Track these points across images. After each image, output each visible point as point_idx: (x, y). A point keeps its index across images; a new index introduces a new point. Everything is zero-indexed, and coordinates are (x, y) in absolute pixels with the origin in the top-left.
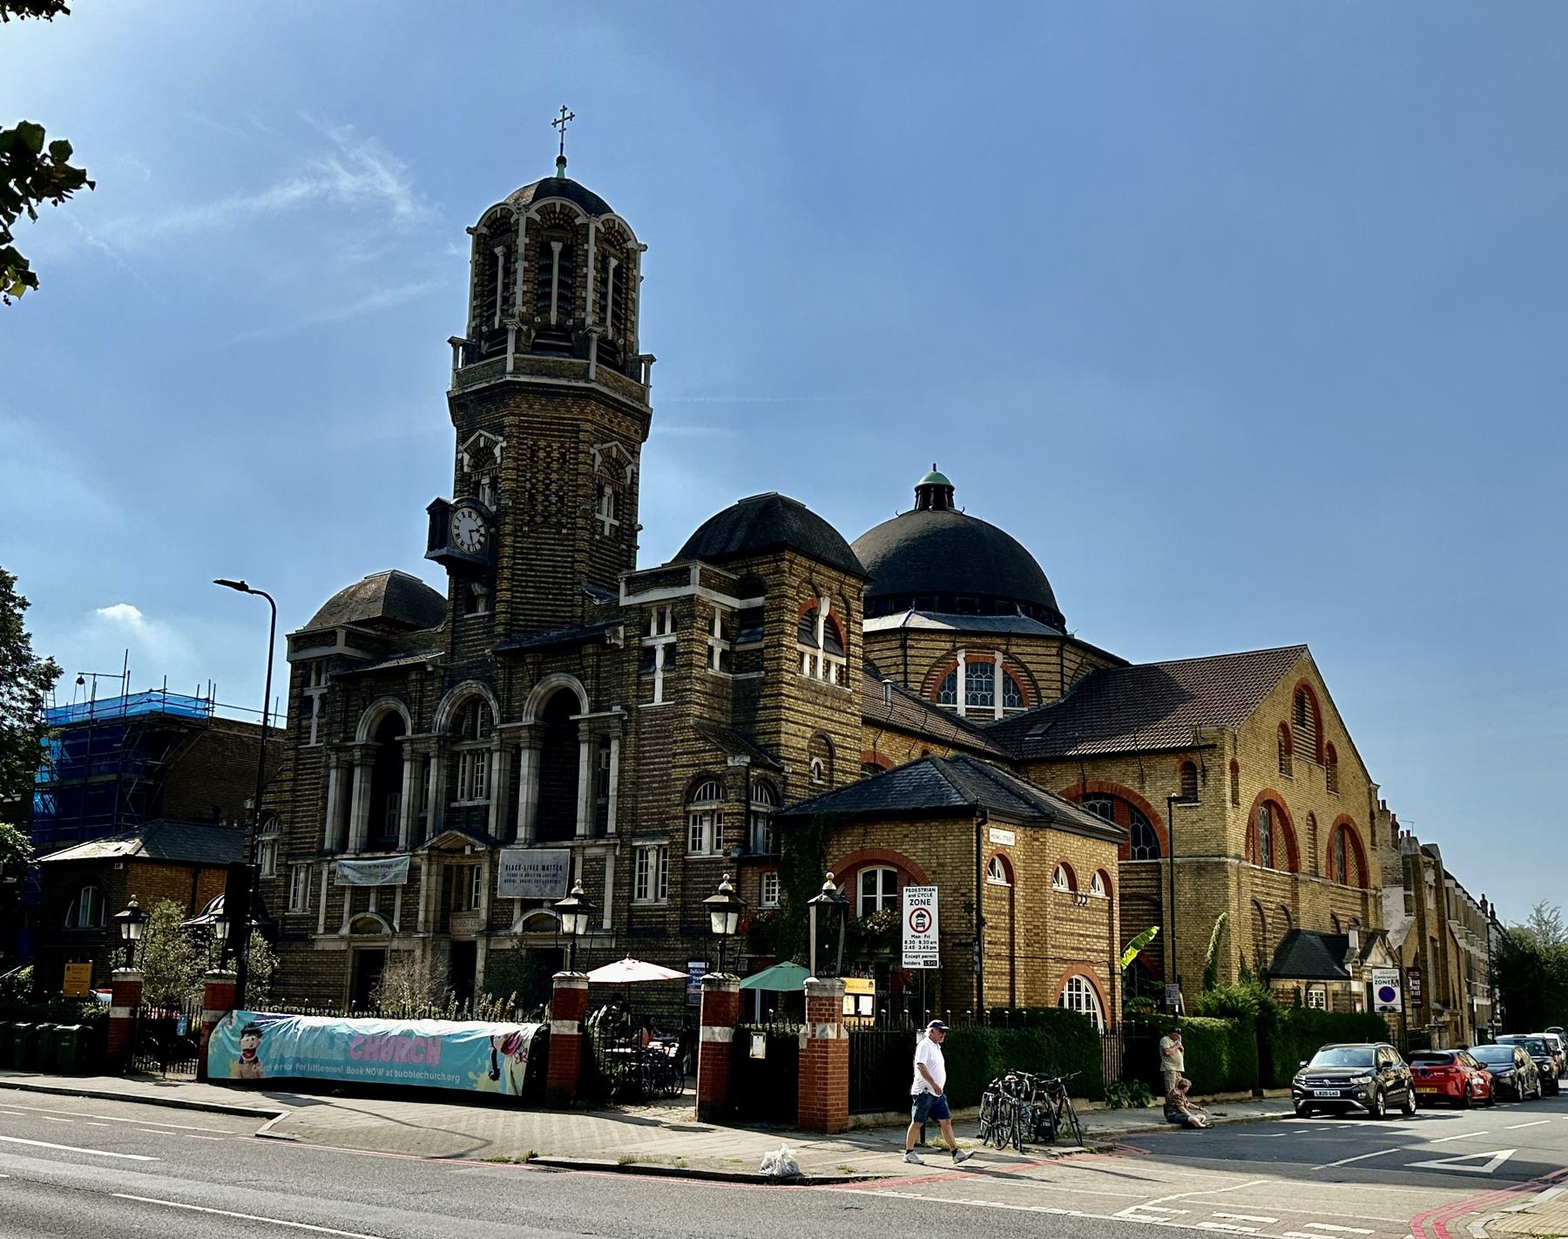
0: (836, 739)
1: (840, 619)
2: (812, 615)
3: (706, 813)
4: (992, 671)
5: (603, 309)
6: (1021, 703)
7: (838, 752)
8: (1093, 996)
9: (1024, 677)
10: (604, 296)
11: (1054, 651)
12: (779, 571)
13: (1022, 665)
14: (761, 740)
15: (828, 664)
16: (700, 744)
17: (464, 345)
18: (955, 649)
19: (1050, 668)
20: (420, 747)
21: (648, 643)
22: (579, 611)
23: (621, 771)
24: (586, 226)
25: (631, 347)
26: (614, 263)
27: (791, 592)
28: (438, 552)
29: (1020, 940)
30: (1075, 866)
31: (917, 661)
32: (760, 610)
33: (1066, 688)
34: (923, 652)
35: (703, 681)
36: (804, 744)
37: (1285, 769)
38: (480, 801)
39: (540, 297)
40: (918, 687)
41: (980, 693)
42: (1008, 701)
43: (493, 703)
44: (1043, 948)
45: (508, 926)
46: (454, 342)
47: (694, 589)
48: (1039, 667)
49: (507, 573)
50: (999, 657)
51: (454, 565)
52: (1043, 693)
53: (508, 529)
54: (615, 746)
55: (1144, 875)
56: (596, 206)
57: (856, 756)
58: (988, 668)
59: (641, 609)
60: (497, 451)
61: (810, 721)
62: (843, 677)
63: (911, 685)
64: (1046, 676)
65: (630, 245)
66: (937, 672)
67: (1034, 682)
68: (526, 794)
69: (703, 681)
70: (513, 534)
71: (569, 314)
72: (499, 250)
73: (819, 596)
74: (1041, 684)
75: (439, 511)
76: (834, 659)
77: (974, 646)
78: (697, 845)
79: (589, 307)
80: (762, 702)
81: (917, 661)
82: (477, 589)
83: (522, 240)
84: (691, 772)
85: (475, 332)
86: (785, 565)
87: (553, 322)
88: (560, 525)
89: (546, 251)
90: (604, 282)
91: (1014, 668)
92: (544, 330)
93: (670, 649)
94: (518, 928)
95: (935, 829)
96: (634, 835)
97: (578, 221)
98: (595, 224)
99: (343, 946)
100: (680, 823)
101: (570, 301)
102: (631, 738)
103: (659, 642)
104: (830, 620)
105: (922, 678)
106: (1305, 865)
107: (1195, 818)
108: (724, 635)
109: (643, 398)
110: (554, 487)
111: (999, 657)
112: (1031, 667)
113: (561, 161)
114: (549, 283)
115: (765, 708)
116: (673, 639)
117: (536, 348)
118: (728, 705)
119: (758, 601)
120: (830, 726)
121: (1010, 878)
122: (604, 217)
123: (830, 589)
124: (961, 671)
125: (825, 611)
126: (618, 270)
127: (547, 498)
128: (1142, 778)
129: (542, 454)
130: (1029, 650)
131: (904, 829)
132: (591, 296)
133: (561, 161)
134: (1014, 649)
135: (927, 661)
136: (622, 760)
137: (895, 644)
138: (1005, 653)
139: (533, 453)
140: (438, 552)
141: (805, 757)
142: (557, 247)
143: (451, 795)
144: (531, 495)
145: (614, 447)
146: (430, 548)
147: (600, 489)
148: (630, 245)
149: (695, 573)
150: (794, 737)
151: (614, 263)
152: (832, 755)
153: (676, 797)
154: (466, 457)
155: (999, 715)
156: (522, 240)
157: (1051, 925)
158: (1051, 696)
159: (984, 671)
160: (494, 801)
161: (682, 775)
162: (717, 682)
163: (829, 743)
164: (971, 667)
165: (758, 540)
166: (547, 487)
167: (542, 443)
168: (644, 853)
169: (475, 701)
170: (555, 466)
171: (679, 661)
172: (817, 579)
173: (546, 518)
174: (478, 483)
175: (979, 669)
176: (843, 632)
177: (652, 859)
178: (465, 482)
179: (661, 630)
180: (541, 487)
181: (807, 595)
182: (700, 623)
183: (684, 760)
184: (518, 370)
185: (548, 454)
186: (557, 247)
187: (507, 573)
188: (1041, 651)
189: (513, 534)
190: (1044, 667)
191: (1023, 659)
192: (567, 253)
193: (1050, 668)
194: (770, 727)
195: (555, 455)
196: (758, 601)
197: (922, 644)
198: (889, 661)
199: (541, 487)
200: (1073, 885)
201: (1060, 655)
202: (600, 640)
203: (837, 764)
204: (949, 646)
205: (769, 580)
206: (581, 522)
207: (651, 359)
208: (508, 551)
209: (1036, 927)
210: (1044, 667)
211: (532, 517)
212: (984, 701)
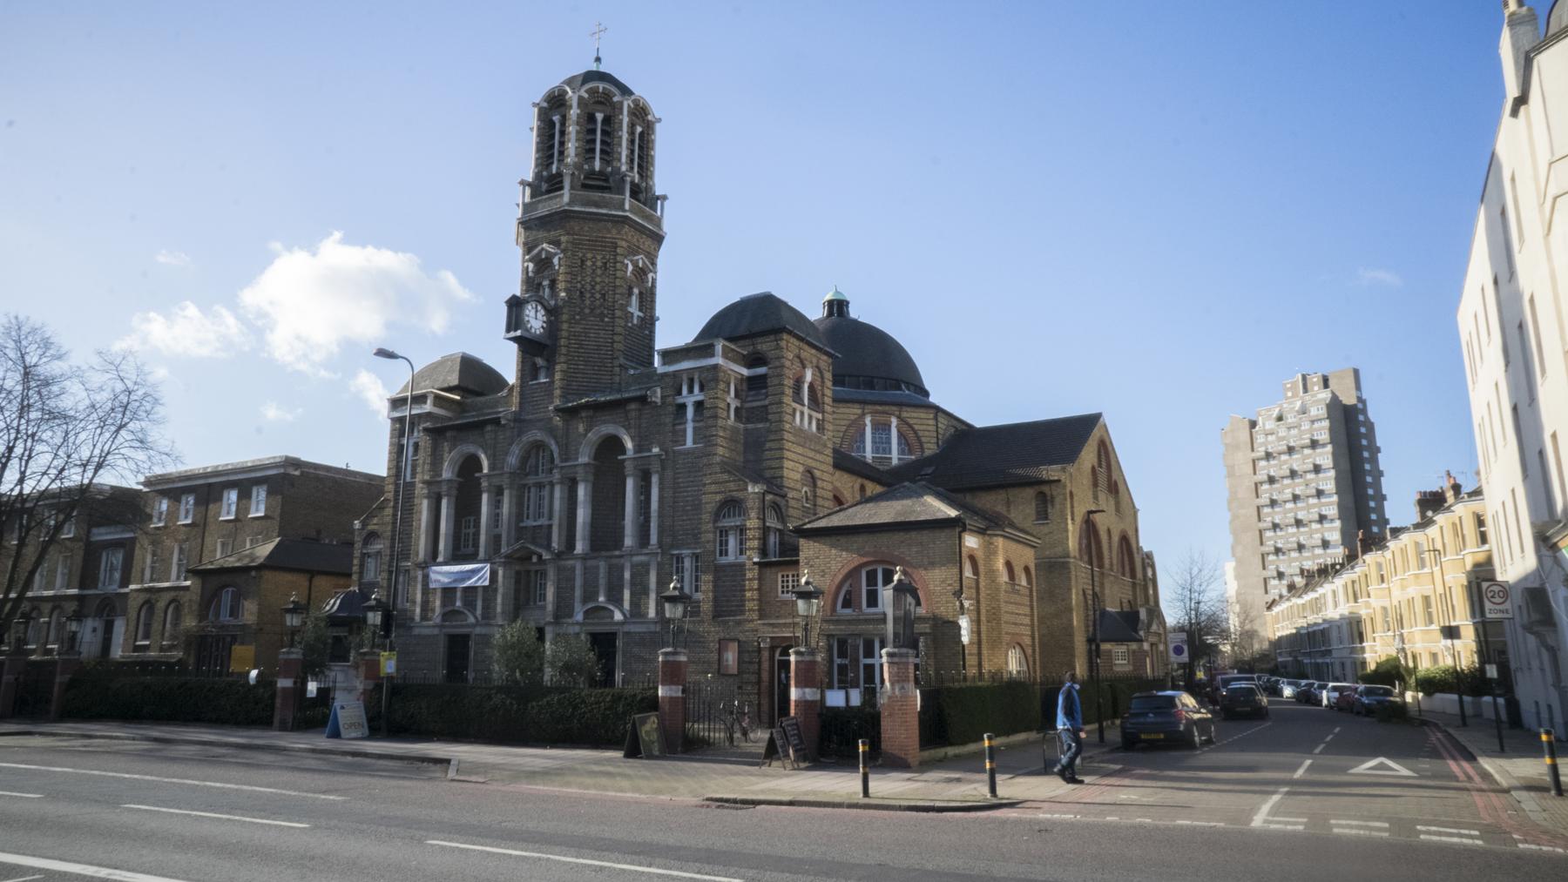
0: (817, 473)
2: (798, 382)
3: (731, 528)
5: (632, 161)
6: (910, 453)
7: (819, 483)
10: (632, 151)
12: (779, 348)
13: (910, 426)
14: (768, 474)
15: (810, 417)
16: (726, 477)
17: (529, 185)
18: (864, 414)
20: (496, 481)
21: (680, 400)
22: (617, 379)
23: (661, 498)
24: (621, 103)
25: (649, 189)
26: (639, 129)
27: (788, 363)
28: (512, 334)
29: (983, 618)
30: (1014, 564)
32: (763, 377)
35: (724, 429)
36: (798, 476)
37: (1096, 498)
38: (543, 521)
39: (587, 152)
41: (882, 444)
42: (901, 452)
43: (554, 447)
44: (999, 624)
45: (571, 616)
46: (523, 183)
47: (718, 360)
50: (894, 421)
51: (528, 347)
53: (565, 317)
56: (626, 91)
57: (830, 487)
59: (675, 374)
60: (556, 261)
61: (802, 460)
62: (820, 427)
66: (852, 430)
67: (918, 438)
68: (582, 515)
69: (724, 429)
70: (569, 322)
72: (556, 118)
73: (804, 367)
75: (515, 305)
76: (815, 414)
77: (877, 412)
78: (724, 552)
80: (768, 445)
82: (540, 361)
83: (574, 112)
84: (719, 497)
85: (538, 176)
86: (783, 344)
89: (591, 118)
91: (905, 428)
92: (591, 174)
93: (699, 405)
94: (579, 617)
95: (925, 536)
96: (673, 547)
97: (615, 99)
98: (627, 103)
99: (436, 631)
100: (711, 536)
101: (608, 153)
102: (669, 473)
103: (689, 399)
104: (811, 386)
106: (1107, 562)
108: (737, 396)
109: (659, 225)
111: (894, 421)
113: (598, 59)
114: (594, 141)
116: (700, 398)
117: (585, 187)
118: (741, 448)
119: (762, 370)
120: (813, 464)
124: (868, 430)
126: (642, 134)
128: (1008, 504)
129: (589, 263)
131: (898, 537)
132: (624, 153)
133: (598, 59)
134: (904, 415)
136: (661, 490)
138: (899, 417)
140: (512, 334)
141: (798, 486)
142: (599, 116)
143: (519, 515)
145: (641, 260)
146: (508, 331)
147: (630, 289)
149: (719, 347)
150: (792, 472)
151: (639, 129)
152: (815, 485)
153: (706, 517)
154: (531, 266)
155: (895, 462)
156: (574, 112)
157: (1004, 608)
158: (931, 449)
160: (556, 522)
161: (711, 500)
162: (734, 430)
163: (813, 478)
165: (754, 324)
166: (593, 287)
167: (589, 255)
168: (680, 559)
169: (539, 446)
170: (599, 272)
171: (707, 413)
172: (804, 355)
174: (540, 284)
175: (881, 428)
177: (687, 563)
178: (531, 283)
179: (691, 391)
180: (588, 287)
181: (797, 364)
182: (722, 386)
183: (713, 488)
184: (571, 202)
186: (599, 116)
187: (564, 350)
189: (569, 322)
192: (607, 120)
194: (774, 464)
195: (599, 264)
196: (762, 370)
199: (588, 287)
201: (936, 418)
202: (643, 400)
203: (819, 492)
205: (771, 354)
206: (618, 313)
207: (664, 198)
208: (564, 334)
212: (884, 451)
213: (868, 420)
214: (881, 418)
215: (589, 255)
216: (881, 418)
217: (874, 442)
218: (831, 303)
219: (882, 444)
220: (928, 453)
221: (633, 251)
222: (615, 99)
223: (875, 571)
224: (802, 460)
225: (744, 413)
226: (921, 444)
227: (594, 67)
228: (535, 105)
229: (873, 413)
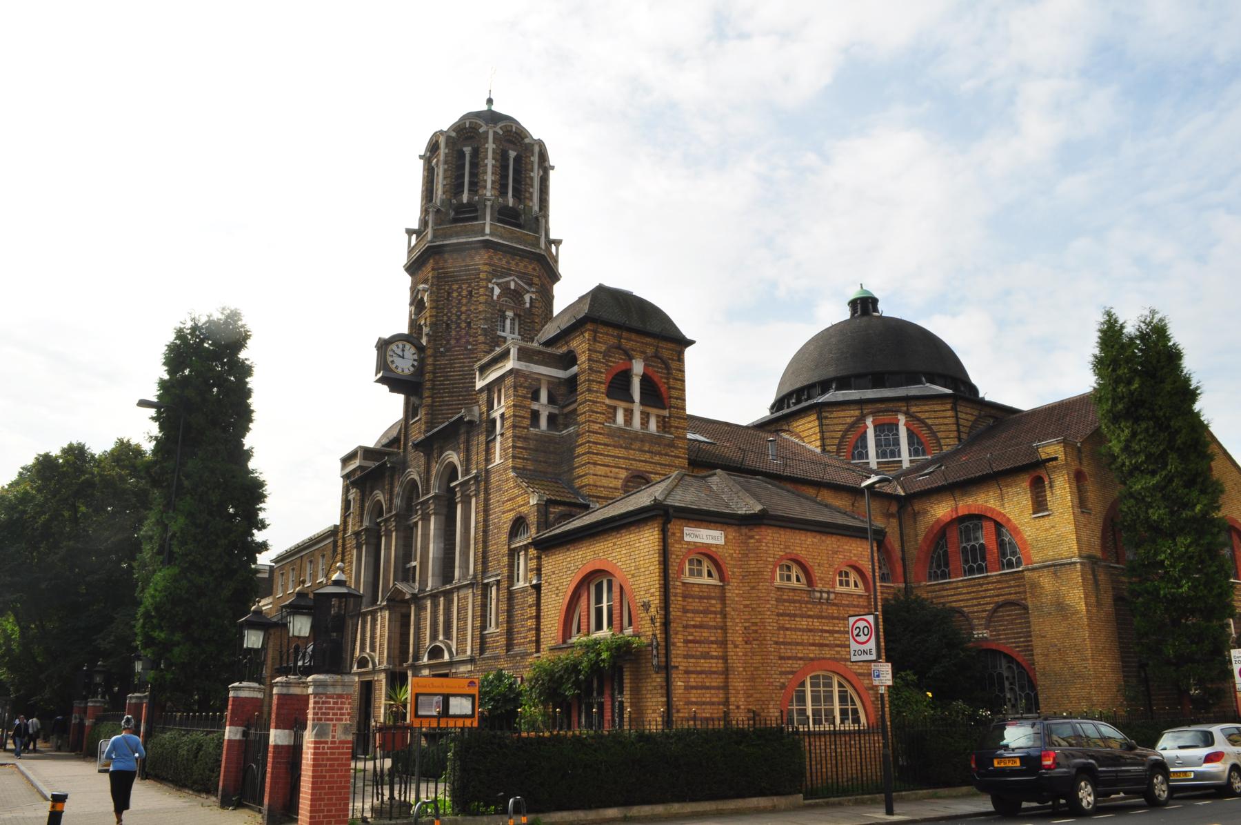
1: (658, 377)
4: (897, 430)
8: (850, 691)
9: (925, 431)
11: (949, 407)
14: (577, 483)
18: (862, 418)
19: (947, 421)
23: (477, 523)
24: (487, 132)
26: (512, 154)
30: (809, 562)
31: (831, 428)
32: (575, 377)
33: (964, 436)
34: (836, 421)
36: (619, 483)
40: (834, 448)
41: (888, 447)
42: (914, 451)
46: (410, 232)
48: (937, 421)
49: (428, 385)
50: (902, 419)
52: (943, 442)
54: (473, 500)
55: (1012, 583)
58: (894, 427)
63: (828, 448)
64: (943, 428)
65: (527, 141)
66: (851, 436)
67: (934, 434)
71: (476, 192)
73: (631, 358)
74: (939, 435)
76: (653, 411)
79: (489, 185)
80: (579, 450)
81: (831, 428)
84: (512, 515)
87: (465, 201)
88: (468, 342)
89: (461, 155)
90: (504, 167)
97: (481, 130)
101: (475, 186)
104: (645, 379)
105: (837, 441)
107: (1048, 526)
108: (552, 400)
110: (463, 317)
111: (902, 419)
112: (929, 422)
113: (490, 101)
115: (579, 456)
120: (649, 468)
121: (722, 579)
122: (501, 124)
123: (644, 352)
124: (870, 433)
125: (638, 367)
126: (518, 160)
127: (458, 325)
129: (455, 294)
130: (927, 408)
133: (490, 101)
134: (913, 409)
135: (841, 427)
137: (814, 417)
138: (907, 414)
139: (449, 294)
142: (467, 150)
144: (448, 325)
148: (527, 141)
151: (512, 154)
155: (906, 465)
159: (890, 430)
164: (879, 428)
166: (459, 318)
167: (455, 287)
170: (464, 301)
173: (458, 340)
175: (886, 430)
176: (663, 389)
180: (454, 318)
185: (460, 294)
187: (428, 385)
188: (937, 407)
190: (941, 421)
191: (923, 416)
192: (476, 153)
193: (947, 421)
195: (465, 293)
197: (835, 414)
198: (811, 432)
199: (454, 318)
200: (810, 582)
201: (954, 409)
204: (857, 413)
208: (429, 368)
209: (755, 624)
210: (941, 421)
211: (448, 341)
212: (893, 454)
213: (869, 422)
214: (885, 418)
215: (455, 287)
216: (885, 418)
217: (878, 445)
218: (853, 304)
219: (888, 447)
220: (946, 449)
221: (497, 273)
222: (481, 130)
223: (602, 583)
224: (622, 463)
225: (561, 420)
226: (938, 440)
227: (484, 107)
228: (421, 157)
229: (873, 413)
